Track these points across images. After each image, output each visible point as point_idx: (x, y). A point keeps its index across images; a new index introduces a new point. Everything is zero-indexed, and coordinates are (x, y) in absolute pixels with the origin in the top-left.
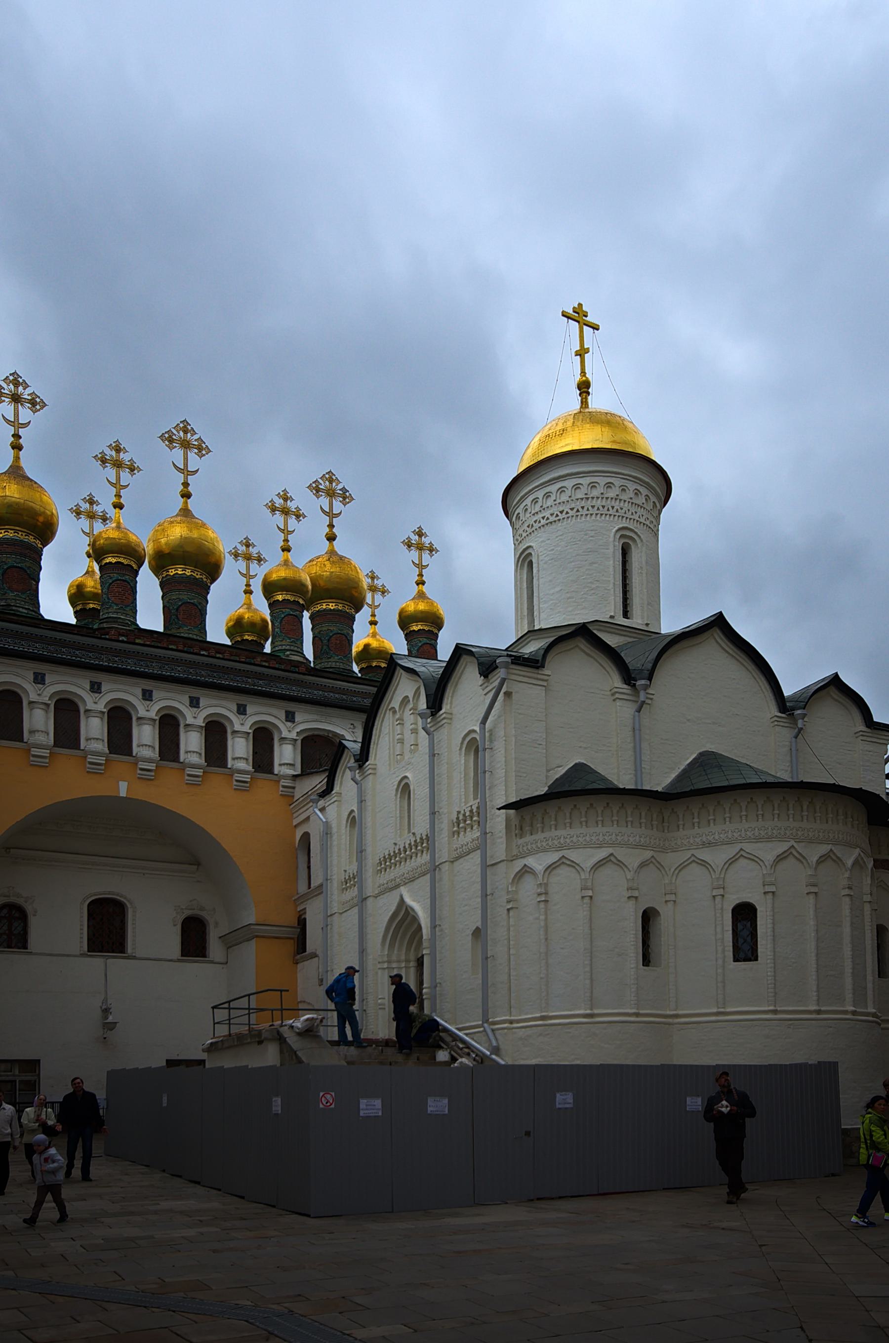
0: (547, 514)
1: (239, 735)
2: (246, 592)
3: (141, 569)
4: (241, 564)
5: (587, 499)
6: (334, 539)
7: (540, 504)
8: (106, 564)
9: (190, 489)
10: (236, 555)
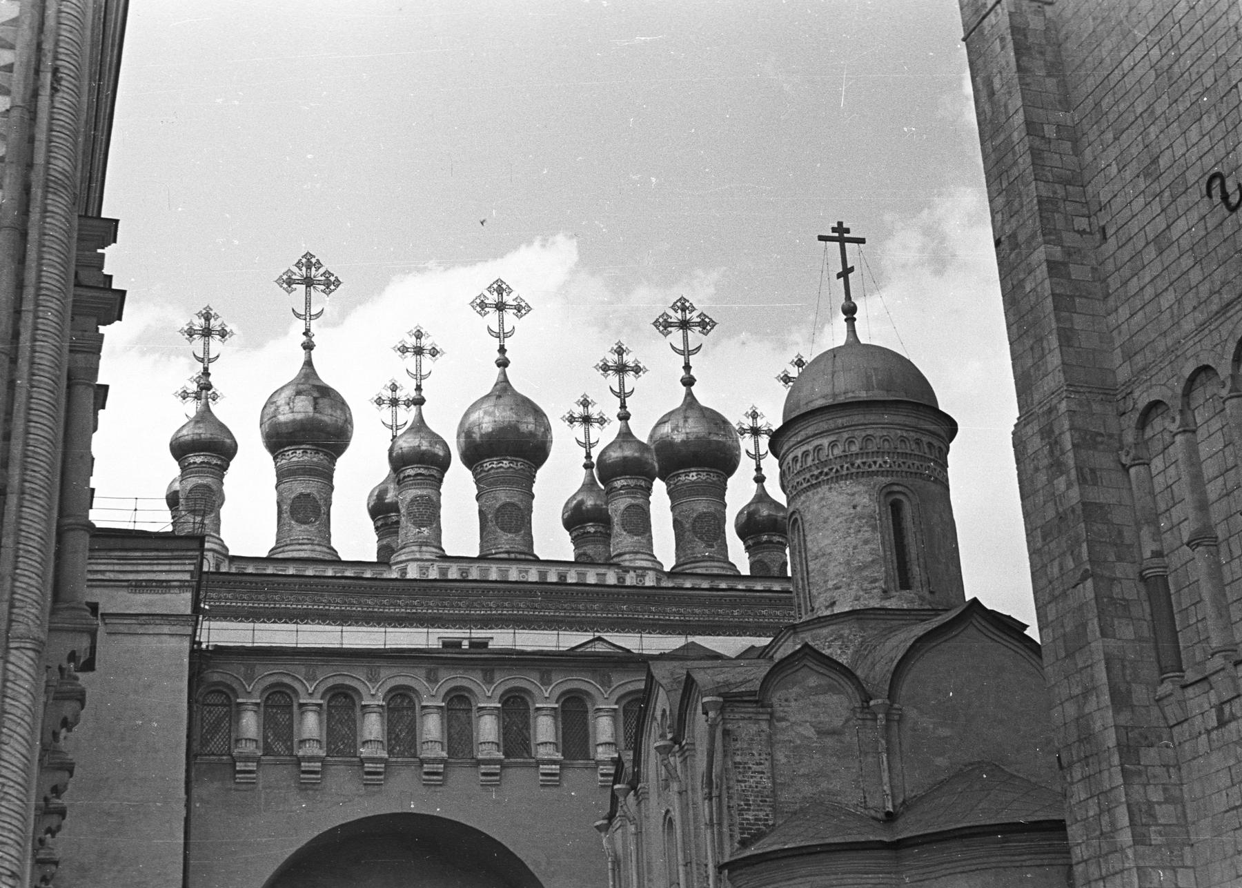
0: (808, 476)
1: (544, 712)
2: (586, 466)
3: (446, 475)
4: (579, 430)
5: (846, 456)
6: (692, 384)
7: (799, 464)
8: (405, 477)
9: (507, 355)
10: (572, 420)
